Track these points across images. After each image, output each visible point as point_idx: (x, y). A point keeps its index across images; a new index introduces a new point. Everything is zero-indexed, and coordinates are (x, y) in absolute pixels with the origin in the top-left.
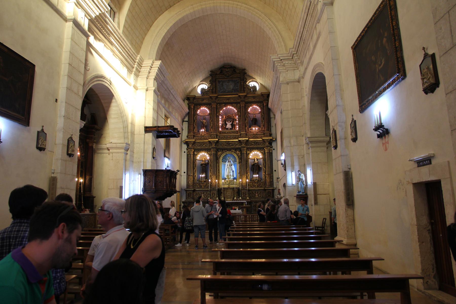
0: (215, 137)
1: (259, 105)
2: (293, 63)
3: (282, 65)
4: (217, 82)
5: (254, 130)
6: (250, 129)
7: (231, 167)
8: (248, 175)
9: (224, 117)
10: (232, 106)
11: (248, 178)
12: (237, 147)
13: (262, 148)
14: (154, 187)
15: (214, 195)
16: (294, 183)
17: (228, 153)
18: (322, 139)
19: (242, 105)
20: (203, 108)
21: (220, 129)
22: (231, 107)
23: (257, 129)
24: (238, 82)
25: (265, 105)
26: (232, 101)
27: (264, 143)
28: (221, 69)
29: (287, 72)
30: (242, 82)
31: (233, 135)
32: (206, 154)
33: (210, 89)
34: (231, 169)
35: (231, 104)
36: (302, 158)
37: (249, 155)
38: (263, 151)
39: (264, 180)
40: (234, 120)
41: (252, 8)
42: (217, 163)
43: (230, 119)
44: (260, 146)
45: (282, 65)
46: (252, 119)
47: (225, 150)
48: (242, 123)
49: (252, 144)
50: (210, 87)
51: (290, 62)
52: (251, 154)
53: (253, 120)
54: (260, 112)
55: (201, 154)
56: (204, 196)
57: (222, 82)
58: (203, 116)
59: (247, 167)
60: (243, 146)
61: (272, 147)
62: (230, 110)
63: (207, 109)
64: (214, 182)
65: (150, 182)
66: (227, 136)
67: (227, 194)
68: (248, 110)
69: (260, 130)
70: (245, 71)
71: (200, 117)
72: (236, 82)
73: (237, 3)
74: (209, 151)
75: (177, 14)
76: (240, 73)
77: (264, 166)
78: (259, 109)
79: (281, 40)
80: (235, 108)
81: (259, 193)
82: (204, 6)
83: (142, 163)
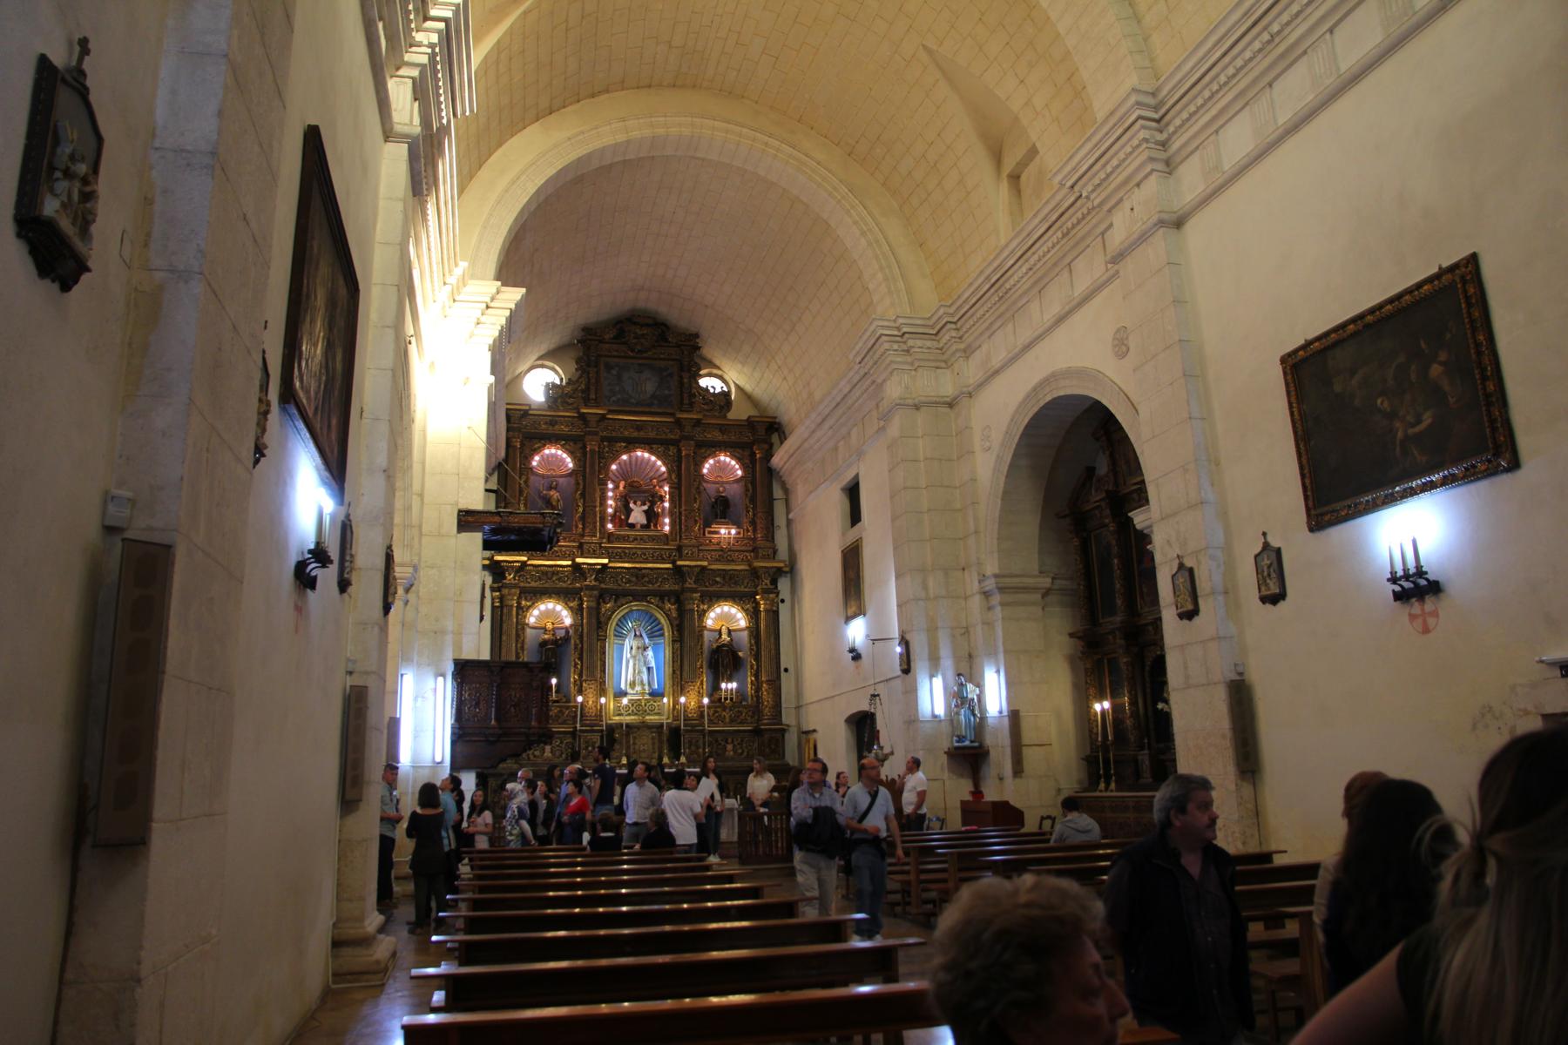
0: (594, 551)
1: (737, 454)
2: (937, 349)
3: (903, 351)
4: (602, 367)
5: (725, 534)
6: (710, 532)
7: (646, 653)
9: (622, 484)
10: (652, 452)
12: (667, 587)
14: (493, 722)
15: (590, 748)
16: (940, 710)
17: (634, 608)
18: (1030, 581)
19: (687, 452)
20: (553, 451)
21: (610, 526)
22: (646, 455)
23: (733, 531)
24: (671, 375)
25: (760, 458)
26: (652, 435)
27: (753, 580)
28: (618, 327)
29: (913, 373)
30: (686, 375)
31: (654, 549)
32: (559, 608)
33: (576, 389)
34: (645, 663)
35: (648, 444)
36: (961, 635)
37: (704, 615)
38: (749, 603)
39: (752, 699)
40: (655, 498)
41: (812, 162)
43: (639, 492)
45: (903, 351)
46: (713, 500)
47: (625, 596)
48: (685, 510)
49: (717, 582)
50: (577, 381)
51: (929, 344)
52: (712, 615)
53: (716, 502)
54: (742, 477)
55: (543, 607)
56: (552, 752)
57: (617, 369)
58: (548, 477)
60: (690, 586)
61: (778, 594)
62: (641, 464)
63: (565, 455)
64: (590, 702)
65: (477, 704)
66: (634, 550)
67: (637, 747)
68: (701, 470)
69: (742, 535)
70: (697, 341)
71: (537, 478)
72: (665, 374)
73: (766, 138)
75: (573, 141)
76: (679, 346)
78: (737, 466)
79: (896, 271)
80: (659, 457)
81: (739, 744)
82: (661, 131)
83: (449, 639)
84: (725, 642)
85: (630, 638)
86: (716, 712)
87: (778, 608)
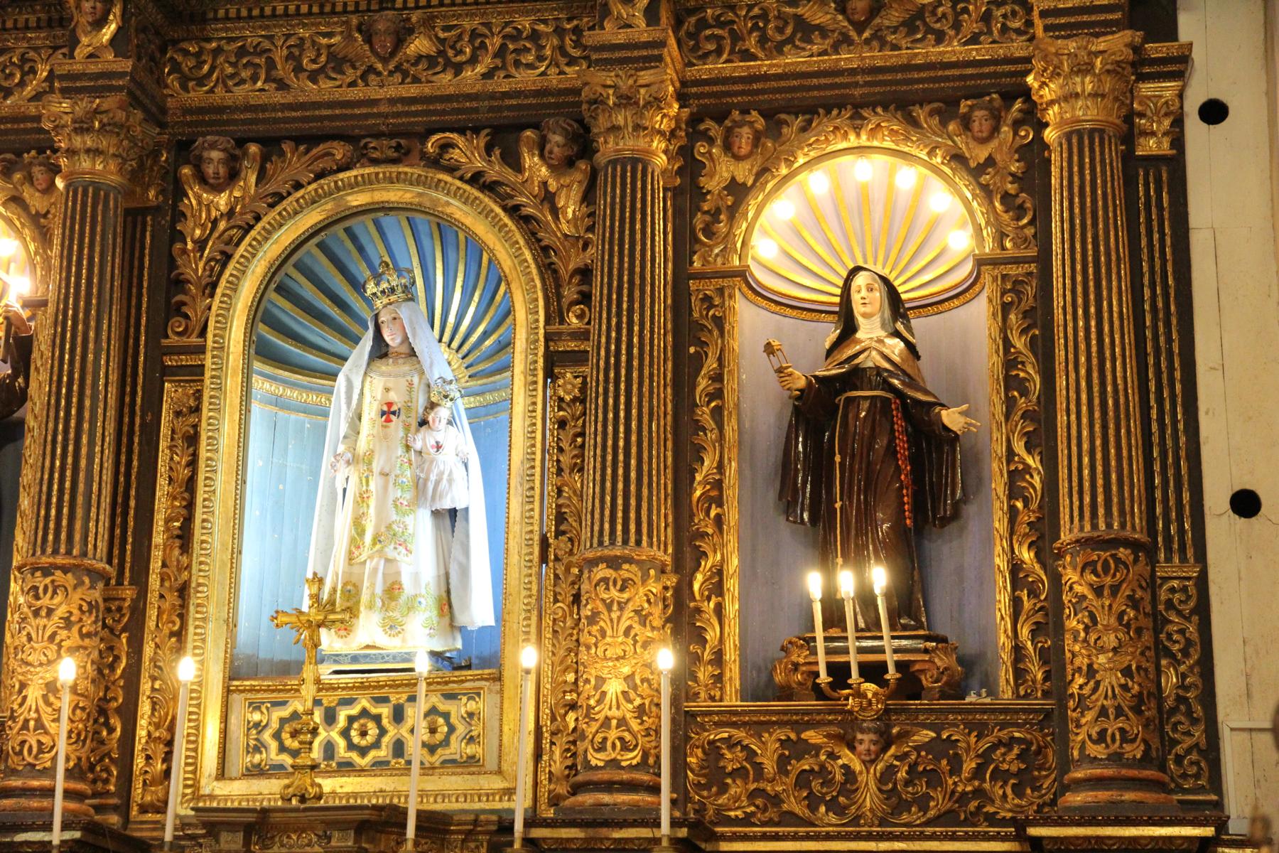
7: (422, 440)
8: (717, 587)
11: (712, 635)
12: (525, 79)
13: (977, 94)
34: (419, 486)
37: (734, 212)
39: (1020, 674)
42: (159, 373)
44: (953, 50)
47: (309, 140)
49: (805, 30)
59: (699, 427)
60: (621, 37)
61: (1178, 67)
74: (38, 172)
77: (1010, 404)
84: (872, 360)
85: (357, 366)
86: (798, 749)
87: (1178, 142)
